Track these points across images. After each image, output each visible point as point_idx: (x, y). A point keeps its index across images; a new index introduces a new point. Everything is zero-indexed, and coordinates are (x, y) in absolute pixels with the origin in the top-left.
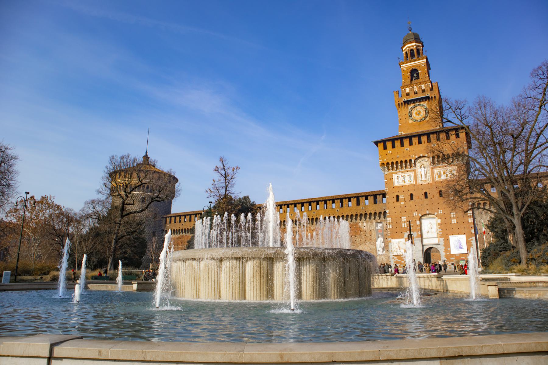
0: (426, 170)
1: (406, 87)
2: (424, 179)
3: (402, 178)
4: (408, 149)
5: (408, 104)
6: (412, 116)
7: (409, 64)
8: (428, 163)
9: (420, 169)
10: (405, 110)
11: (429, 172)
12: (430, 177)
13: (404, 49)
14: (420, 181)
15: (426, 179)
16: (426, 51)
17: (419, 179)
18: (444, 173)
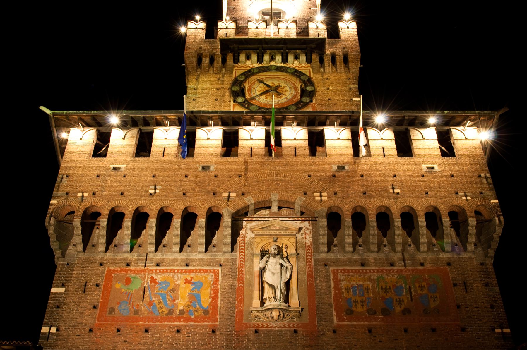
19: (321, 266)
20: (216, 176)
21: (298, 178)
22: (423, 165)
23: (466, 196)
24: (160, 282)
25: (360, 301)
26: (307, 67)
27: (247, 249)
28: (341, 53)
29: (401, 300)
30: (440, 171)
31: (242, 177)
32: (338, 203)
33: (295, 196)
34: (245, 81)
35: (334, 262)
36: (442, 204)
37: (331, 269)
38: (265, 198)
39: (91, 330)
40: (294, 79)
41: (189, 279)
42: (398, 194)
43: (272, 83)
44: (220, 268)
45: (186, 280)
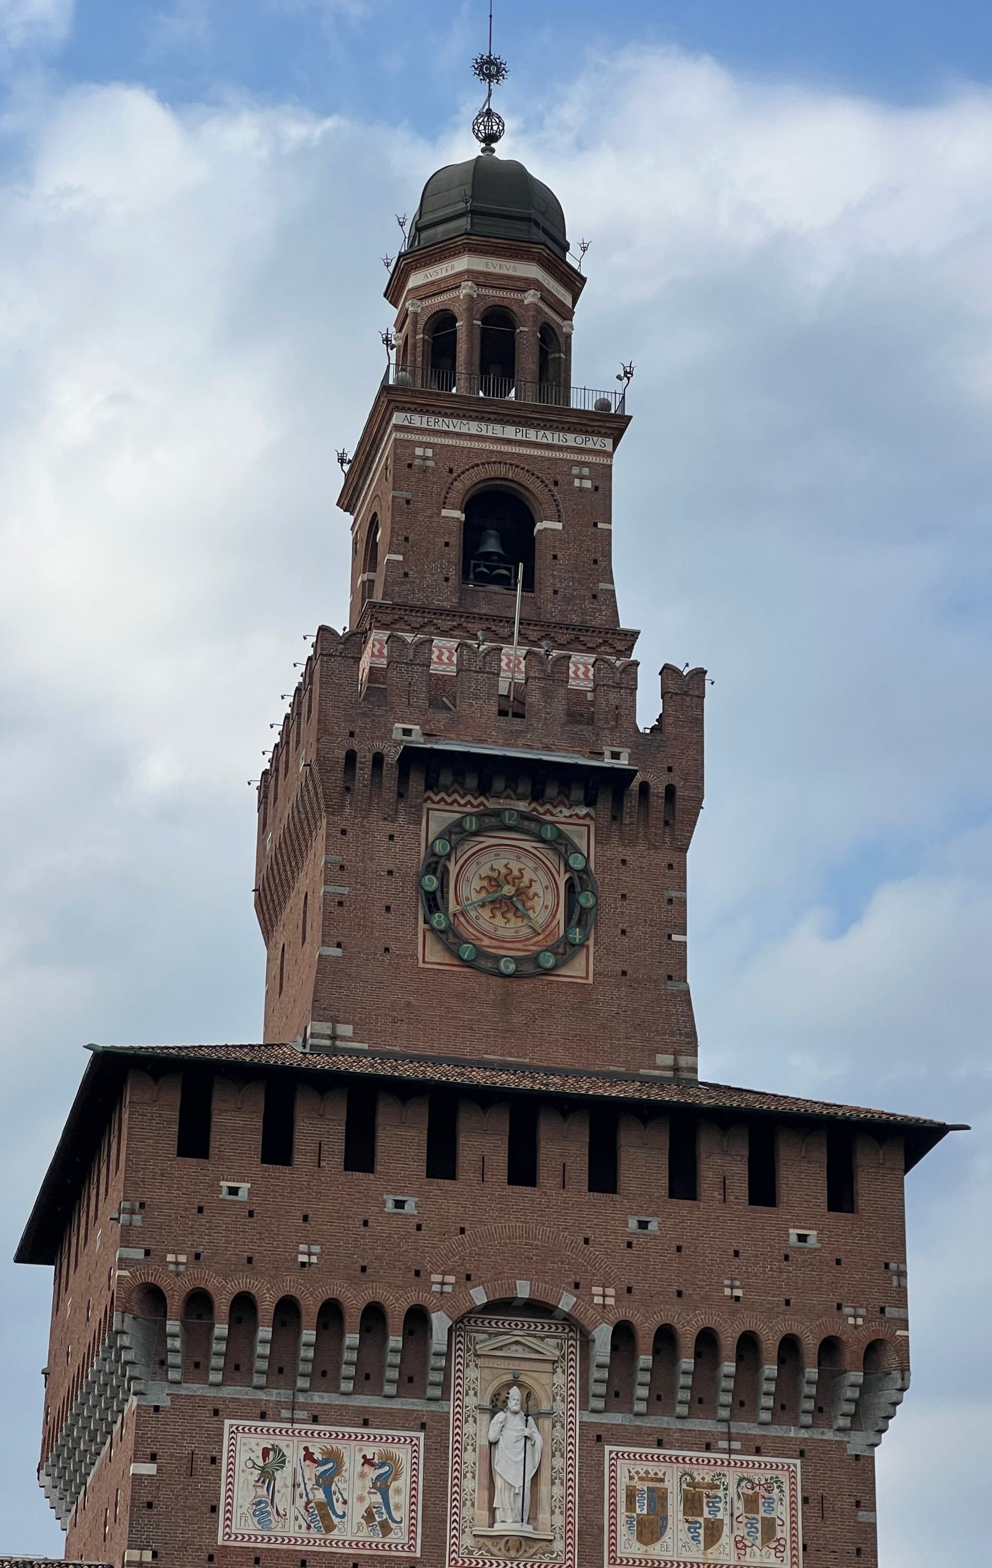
0: (538, 1437)
1: (417, 620)
2: (508, 1524)
3: (312, 1472)
4: (410, 1208)
5: (431, 785)
6: (453, 907)
7: (473, 427)
8: (559, 1379)
9: (487, 1416)
10: (390, 828)
11: (559, 1462)
13: (415, 280)
15: (527, 1530)
16: (628, 374)
17: (466, 1512)
18: (692, 1504)
20: (419, 1228)
22: (791, 1231)
23: (855, 1316)
26: (584, 817)
27: (467, 1394)
28: (662, 790)
31: (467, 1232)
33: (559, 1292)
34: (448, 857)
36: (811, 1331)
37: (608, 1448)
39: (211, 1558)
40: (551, 858)
41: (369, 1457)
42: (737, 1299)
43: (506, 866)
44: (421, 1435)
45: (364, 1457)
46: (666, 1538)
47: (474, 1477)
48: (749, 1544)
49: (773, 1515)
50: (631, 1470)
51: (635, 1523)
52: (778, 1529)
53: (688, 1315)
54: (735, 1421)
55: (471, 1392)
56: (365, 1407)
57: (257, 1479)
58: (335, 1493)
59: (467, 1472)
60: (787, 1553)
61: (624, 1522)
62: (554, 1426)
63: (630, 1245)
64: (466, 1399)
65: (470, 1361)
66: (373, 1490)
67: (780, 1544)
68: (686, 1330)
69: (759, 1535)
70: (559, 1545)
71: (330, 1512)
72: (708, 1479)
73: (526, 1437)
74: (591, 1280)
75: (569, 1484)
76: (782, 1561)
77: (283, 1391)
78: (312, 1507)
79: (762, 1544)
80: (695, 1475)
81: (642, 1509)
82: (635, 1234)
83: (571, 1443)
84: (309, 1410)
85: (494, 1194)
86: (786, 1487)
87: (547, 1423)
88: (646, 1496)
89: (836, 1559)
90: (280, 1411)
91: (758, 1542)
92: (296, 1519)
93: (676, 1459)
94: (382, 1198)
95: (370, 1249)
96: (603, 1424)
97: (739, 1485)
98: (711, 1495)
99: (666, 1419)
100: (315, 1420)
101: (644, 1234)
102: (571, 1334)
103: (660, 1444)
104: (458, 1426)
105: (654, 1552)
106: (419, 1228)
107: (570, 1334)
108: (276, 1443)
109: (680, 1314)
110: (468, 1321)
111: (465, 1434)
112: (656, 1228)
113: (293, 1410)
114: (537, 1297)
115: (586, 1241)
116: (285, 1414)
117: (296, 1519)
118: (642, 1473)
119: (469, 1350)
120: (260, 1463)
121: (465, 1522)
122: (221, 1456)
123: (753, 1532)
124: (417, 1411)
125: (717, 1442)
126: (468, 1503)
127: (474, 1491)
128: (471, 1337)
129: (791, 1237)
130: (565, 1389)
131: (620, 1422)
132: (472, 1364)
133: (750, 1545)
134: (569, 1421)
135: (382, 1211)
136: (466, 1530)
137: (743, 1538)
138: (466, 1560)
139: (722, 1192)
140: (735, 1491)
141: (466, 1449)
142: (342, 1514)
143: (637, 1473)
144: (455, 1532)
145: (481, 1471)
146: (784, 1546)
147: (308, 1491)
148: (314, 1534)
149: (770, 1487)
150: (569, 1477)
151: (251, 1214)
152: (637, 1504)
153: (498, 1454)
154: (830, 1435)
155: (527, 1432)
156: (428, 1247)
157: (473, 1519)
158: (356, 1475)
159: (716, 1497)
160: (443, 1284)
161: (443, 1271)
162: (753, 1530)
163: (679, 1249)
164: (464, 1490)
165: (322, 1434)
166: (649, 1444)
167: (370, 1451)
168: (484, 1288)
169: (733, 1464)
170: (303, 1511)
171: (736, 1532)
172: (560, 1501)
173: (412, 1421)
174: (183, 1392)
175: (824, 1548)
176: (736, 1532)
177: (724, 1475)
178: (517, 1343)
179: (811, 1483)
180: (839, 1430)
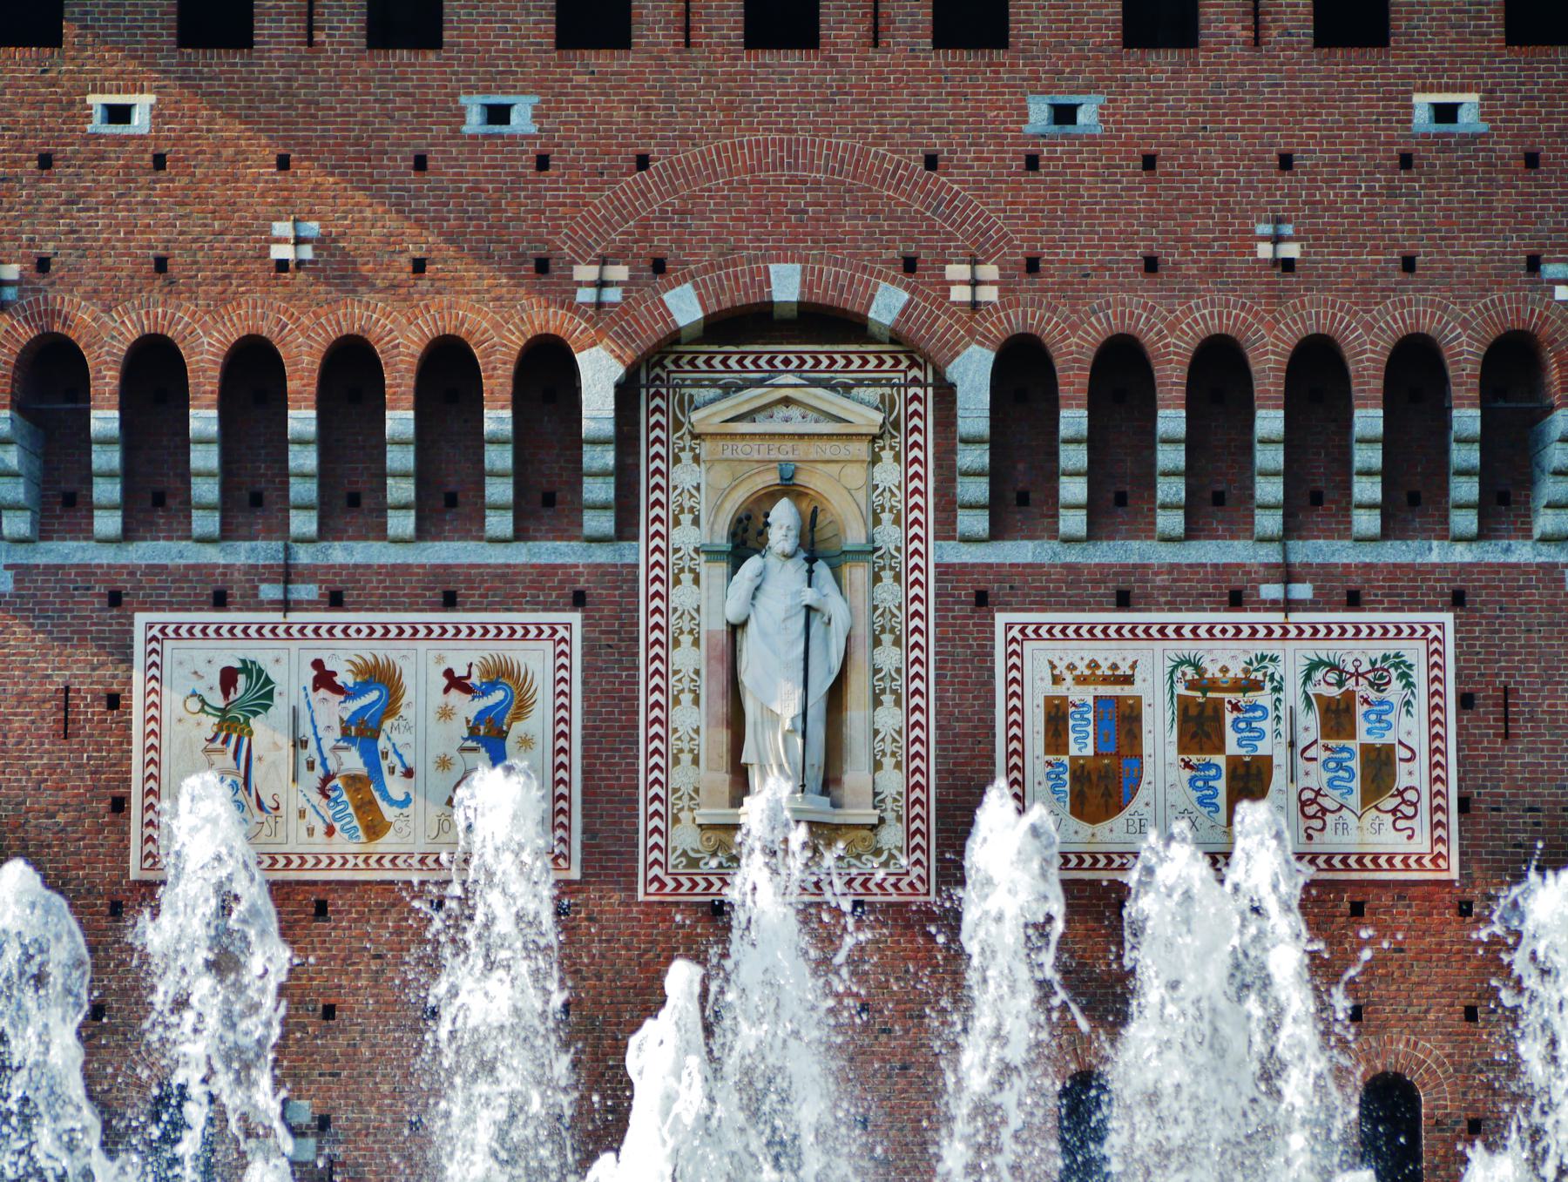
0: (836, 607)
3: (331, 712)
4: (522, 120)
8: (889, 473)
9: (722, 568)
11: (889, 657)
12: (909, 763)
14: (685, 837)
17: (682, 777)
19: (963, 603)
20: (543, 163)
21: (884, 179)
24: (350, 683)
25: (1100, 777)
29: (1254, 771)
30: (1483, 135)
31: (653, 165)
32: (1042, 318)
33: (868, 281)
35: (1011, 588)
36: (1465, 324)
37: (1001, 619)
38: (746, 294)
41: (460, 671)
42: (1288, 265)
44: (575, 618)
45: (449, 673)
46: (1137, 804)
47: (696, 701)
48: (1327, 803)
49: (1390, 738)
50: (1056, 662)
51: (1067, 777)
52: (1402, 769)
53: (1171, 312)
54: (1300, 538)
55: (686, 518)
56: (447, 567)
57: (210, 736)
58: (385, 755)
59: (682, 691)
60: (1422, 823)
61: (1042, 778)
62: (877, 578)
63: (1032, 163)
64: (677, 537)
65: (682, 449)
66: (469, 744)
67: (1404, 801)
68: (1167, 346)
69: (1356, 784)
70: (892, 836)
71: (377, 795)
72: (1236, 671)
73: (809, 609)
74: (944, 248)
75: (913, 703)
76: (1410, 837)
77: (261, 544)
78: (335, 789)
79: (1365, 802)
80: (1206, 663)
81: (1082, 745)
82: (1043, 136)
83: (916, 614)
84: (322, 581)
85: (716, 73)
86: (1420, 676)
87: (858, 574)
88: (1090, 716)
89: (1537, 824)
90: (256, 588)
91: (1354, 800)
92: (302, 814)
93: (1162, 631)
94: (456, 102)
95: (433, 219)
96: (990, 566)
97: (1308, 677)
98: (1242, 703)
99: (1135, 544)
100: (335, 601)
101: (1065, 136)
102: (915, 372)
103: (1124, 601)
104: (657, 594)
105: (1108, 837)
106: (543, 163)
107: (910, 375)
108: (251, 656)
109: (1153, 308)
110: (676, 362)
111: (675, 610)
112: (1095, 119)
113: (287, 581)
114: (818, 296)
115: (931, 162)
116: (270, 591)
117: (302, 814)
118: (1082, 669)
119: (678, 425)
120: (219, 702)
121: (680, 798)
122: (130, 691)
123: (1342, 779)
124: (563, 566)
125: (1256, 589)
126: (686, 758)
127: (697, 731)
128: (682, 397)
129: (1417, 112)
130: (901, 496)
131: (1029, 560)
132: (686, 456)
133: (1335, 806)
134: (911, 564)
135: (456, 133)
136: (681, 815)
137: (1318, 793)
138: (683, 879)
139: (1250, 22)
140: (1300, 691)
141: (677, 643)
142: (402, 797)
143: (1071, 667)
144: (656, 821)
145: (712, 688)
146: (1414, 805)
147: (327, 753)
148: (342, 843)
149: (1381, 677)
150: (912, 688)
151: (159, 162)
152: (1072, 736)
153: (750, 645)
154: (1523, 553)
155: (809, 596)
156: (564, 204)
157: (697, 791)
158: (433, 716)
159: (1254, 707)
160: (601, 284)
161: (598, 256)
162: (1341, 773)
163: (1149, 162)
164: (675, 730)
165: (351, 631)
166: (1097, 603)
167: (463, 656)
168: (696, 286)
169: (1293, 632)
170: (316, 798)
171: (1303, 782)
172: (894, 740)
173: (553, 588)
174: (41, 560)
175: (1509, 803)
176: (1303, 782)
177: (1273, 659)
178: (787, 401)
179: (1480, 661)
180: (1545, 539)
